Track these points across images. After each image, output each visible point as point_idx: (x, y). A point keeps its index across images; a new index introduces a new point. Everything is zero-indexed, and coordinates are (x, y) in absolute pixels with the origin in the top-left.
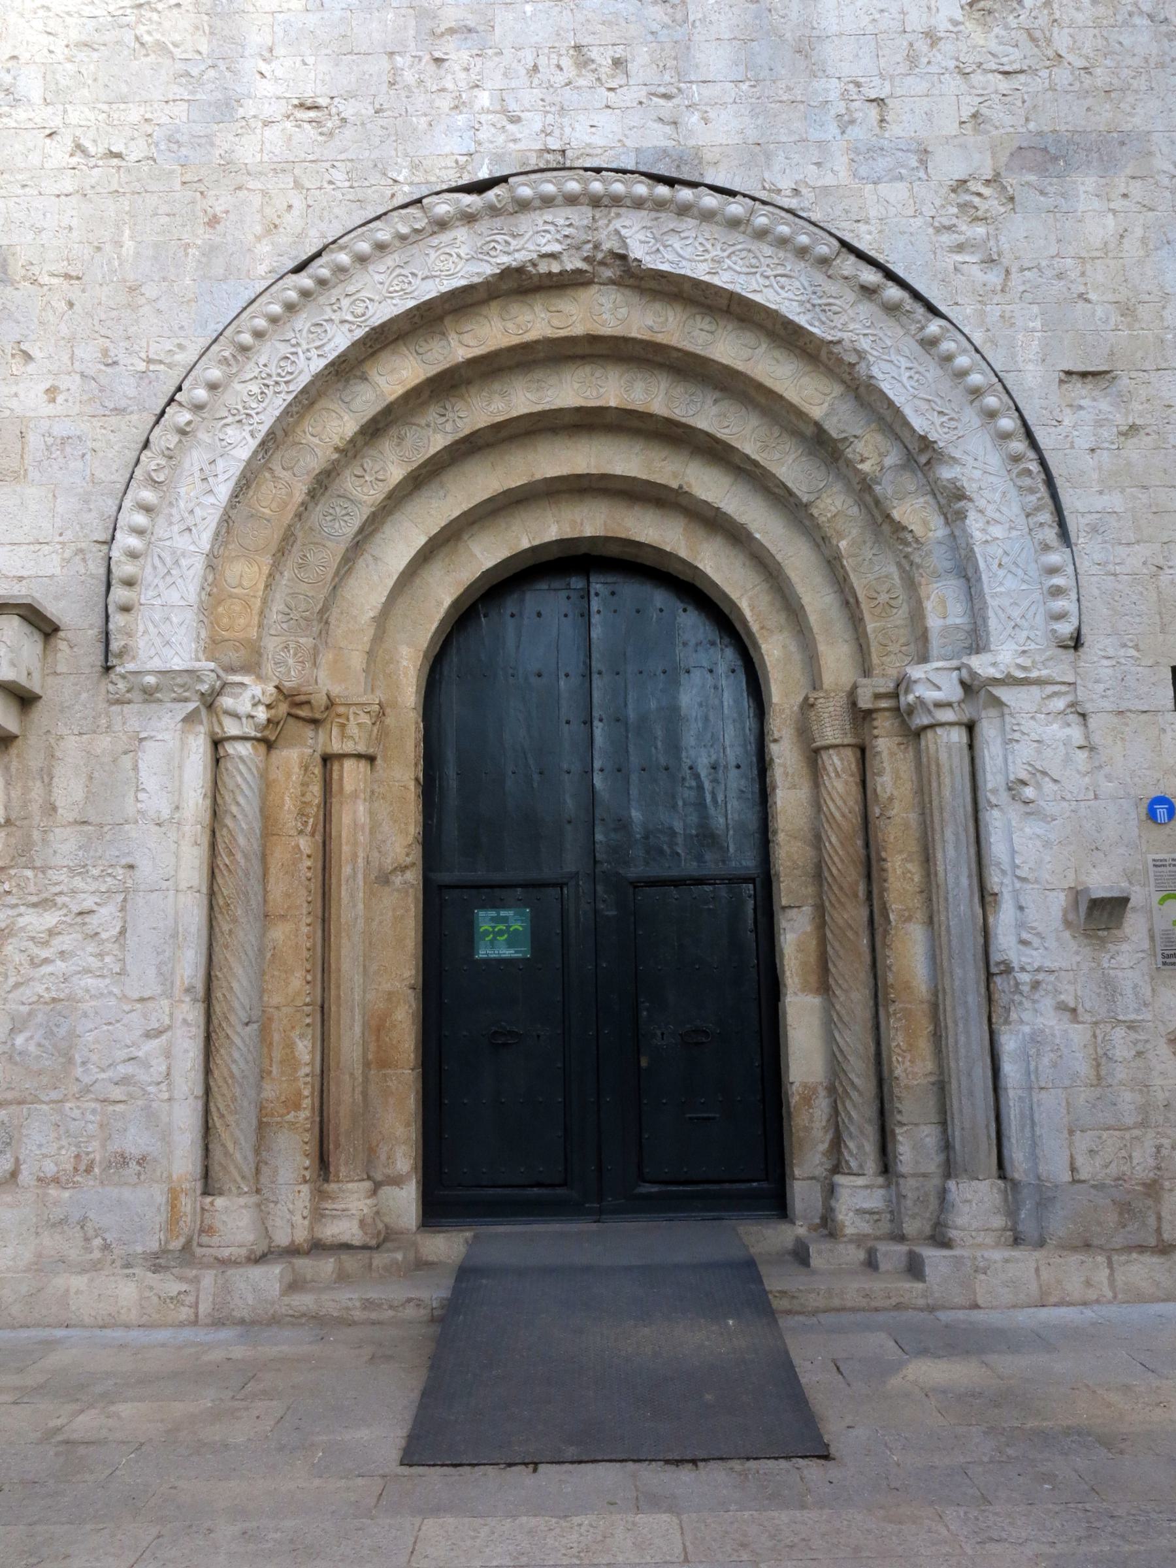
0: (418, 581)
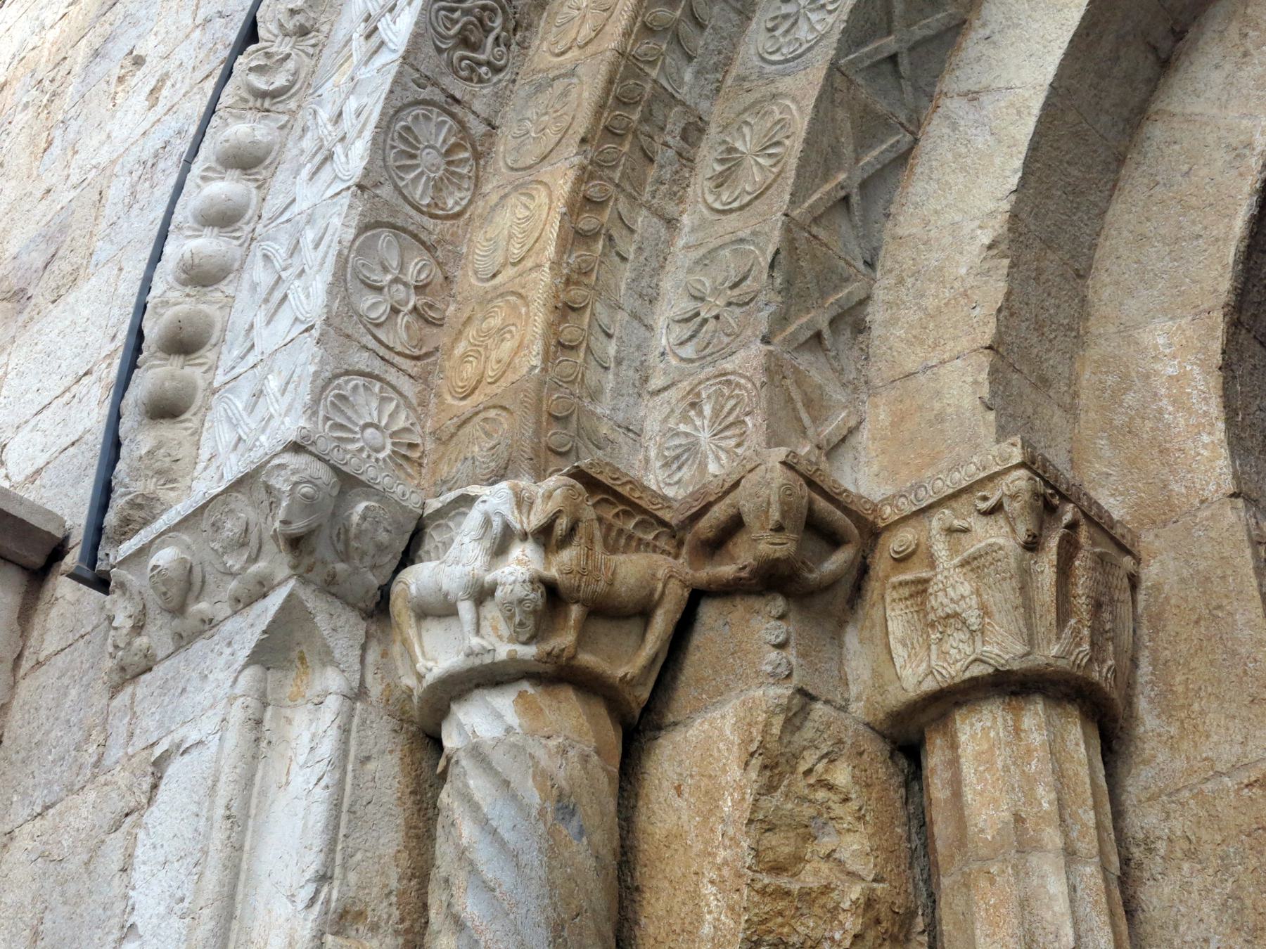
0: (1156, 132)
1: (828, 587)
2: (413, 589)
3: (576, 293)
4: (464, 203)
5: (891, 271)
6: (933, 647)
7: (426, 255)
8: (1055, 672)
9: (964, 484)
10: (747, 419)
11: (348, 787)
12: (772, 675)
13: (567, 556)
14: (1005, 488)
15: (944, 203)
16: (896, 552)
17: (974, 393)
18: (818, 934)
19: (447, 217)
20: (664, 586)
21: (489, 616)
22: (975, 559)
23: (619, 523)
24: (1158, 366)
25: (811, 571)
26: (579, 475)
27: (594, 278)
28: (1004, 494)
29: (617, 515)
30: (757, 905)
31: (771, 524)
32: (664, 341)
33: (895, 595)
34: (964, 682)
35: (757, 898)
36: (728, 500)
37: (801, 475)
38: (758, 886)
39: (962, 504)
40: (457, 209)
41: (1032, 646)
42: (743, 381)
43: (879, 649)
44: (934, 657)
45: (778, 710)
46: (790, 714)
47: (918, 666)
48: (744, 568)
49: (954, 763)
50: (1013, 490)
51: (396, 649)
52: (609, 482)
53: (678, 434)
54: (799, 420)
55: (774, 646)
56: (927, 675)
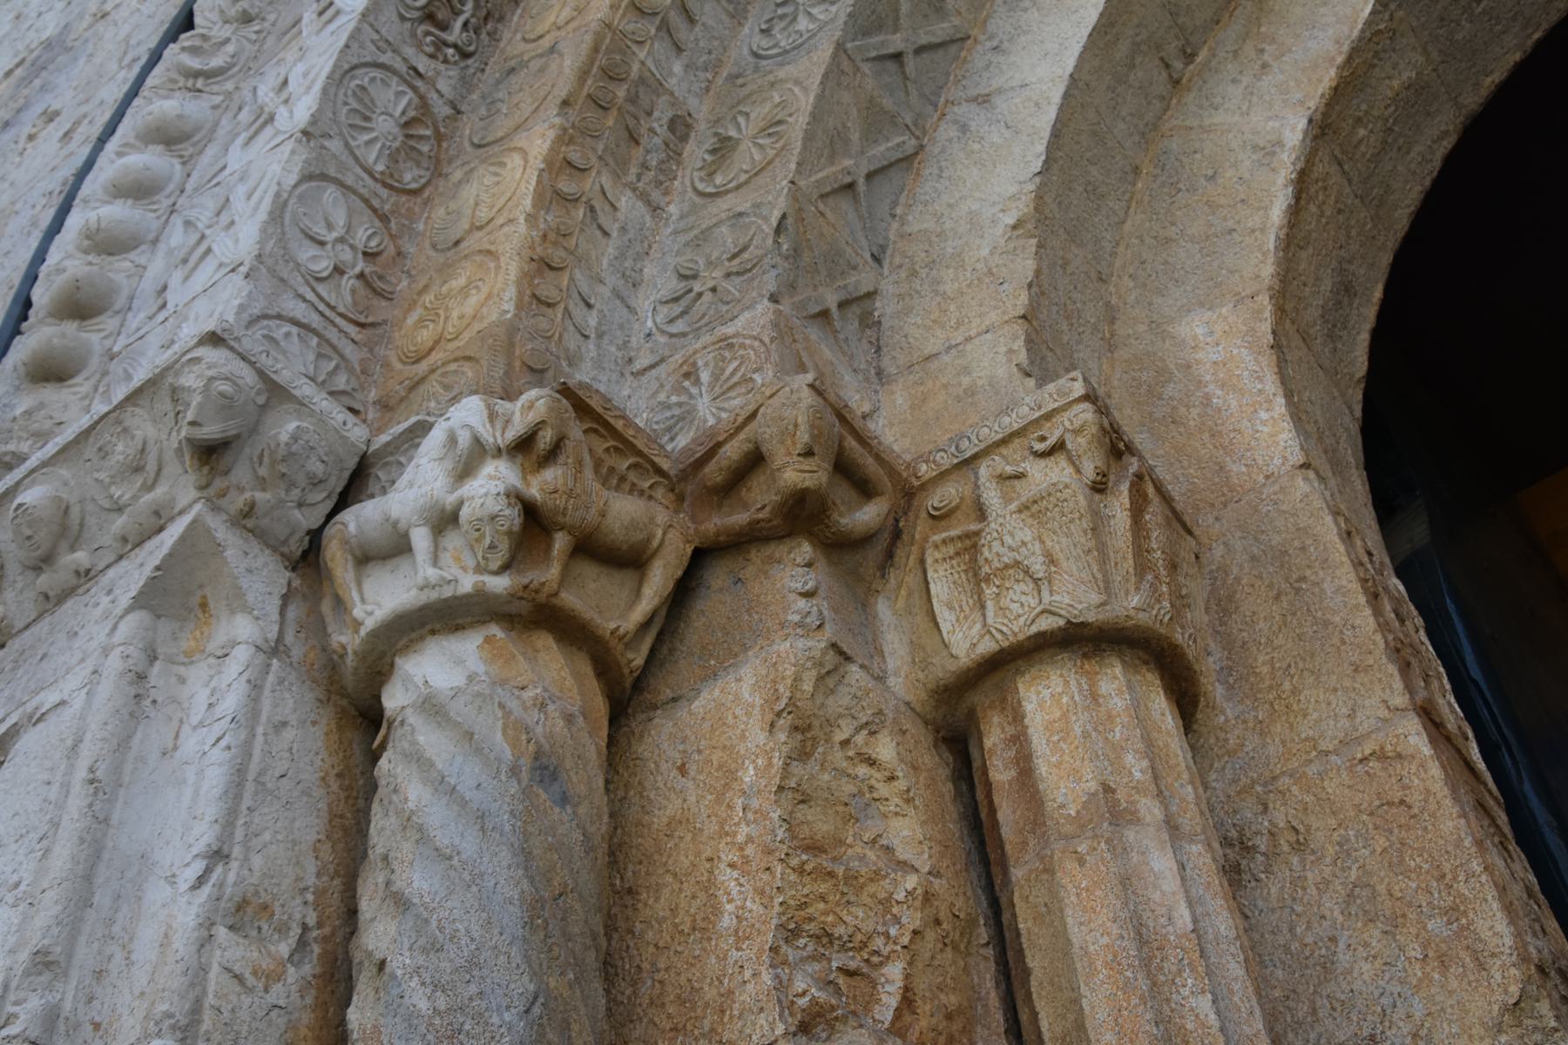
1: (863, 541)
2: (352, 528)
4: (423, 181)
5: (900, 266)
6: (990, 604)
7: (377, 223)
8: (1137, 627)
9: (1016, 426)
10: (755, 376)
11: (257, 753)
12: (798, 625)
13: (551, 475)
14: (1067, 424)
15: (957, 195)
17: (1010, 361)
18: (868, 926)
20: (664, 534)
21: (450, 546)
22: (1035, 502)
24: (1200, 355)
25: (841, 515)
26: (566, 391)
28: (1066, 430)
29: (607, 450)
30: (793, 885)
31: (799, 448)
32: (650, 324)
33: (938, 555)
34: (1029, 638)
35: (793, 877)
36: (742, 436)
37: (831, 405)
38: (795, 862)
39: (1015, 449)
40: (414, 186)
41: (1109, 596)
42: (747, 342)
43: (918, 618)
44: (990, 613)
45: (809, 664)
46: (823, 671)
47: (970, 628)
48: (763, 507)
49: (1020, 740)
50: (1077, 423)
51: (326, 607)
52: (600, 410)
53: (669, 407)
55: (801, 594)
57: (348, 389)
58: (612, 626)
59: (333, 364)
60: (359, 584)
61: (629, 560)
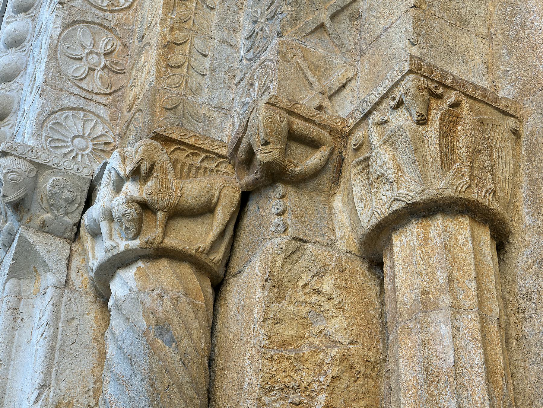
3: (179, 36)
7: (109, 34)
8: (446, 198)
11: (59, 336)
12: (275, 232)
13: (150, 184)
16: (354, 145)
19: (122, 10)
23: (189, 161)
27: (191, 24)
30: (268, 367)
34: (390, 215)
35: (268, 363)
38: (268, 356)
40: (127, 4)
47: (368, 211)
49: (393, 267)
54: (307, 79)
56: (372, 216)
57: (104, 133)
58: (196, 247)
59: (94, 122)
60: (93, 247)
61: (206, 210)
